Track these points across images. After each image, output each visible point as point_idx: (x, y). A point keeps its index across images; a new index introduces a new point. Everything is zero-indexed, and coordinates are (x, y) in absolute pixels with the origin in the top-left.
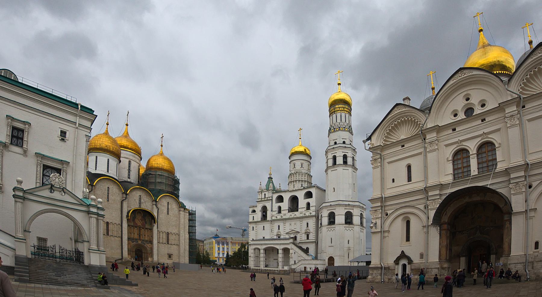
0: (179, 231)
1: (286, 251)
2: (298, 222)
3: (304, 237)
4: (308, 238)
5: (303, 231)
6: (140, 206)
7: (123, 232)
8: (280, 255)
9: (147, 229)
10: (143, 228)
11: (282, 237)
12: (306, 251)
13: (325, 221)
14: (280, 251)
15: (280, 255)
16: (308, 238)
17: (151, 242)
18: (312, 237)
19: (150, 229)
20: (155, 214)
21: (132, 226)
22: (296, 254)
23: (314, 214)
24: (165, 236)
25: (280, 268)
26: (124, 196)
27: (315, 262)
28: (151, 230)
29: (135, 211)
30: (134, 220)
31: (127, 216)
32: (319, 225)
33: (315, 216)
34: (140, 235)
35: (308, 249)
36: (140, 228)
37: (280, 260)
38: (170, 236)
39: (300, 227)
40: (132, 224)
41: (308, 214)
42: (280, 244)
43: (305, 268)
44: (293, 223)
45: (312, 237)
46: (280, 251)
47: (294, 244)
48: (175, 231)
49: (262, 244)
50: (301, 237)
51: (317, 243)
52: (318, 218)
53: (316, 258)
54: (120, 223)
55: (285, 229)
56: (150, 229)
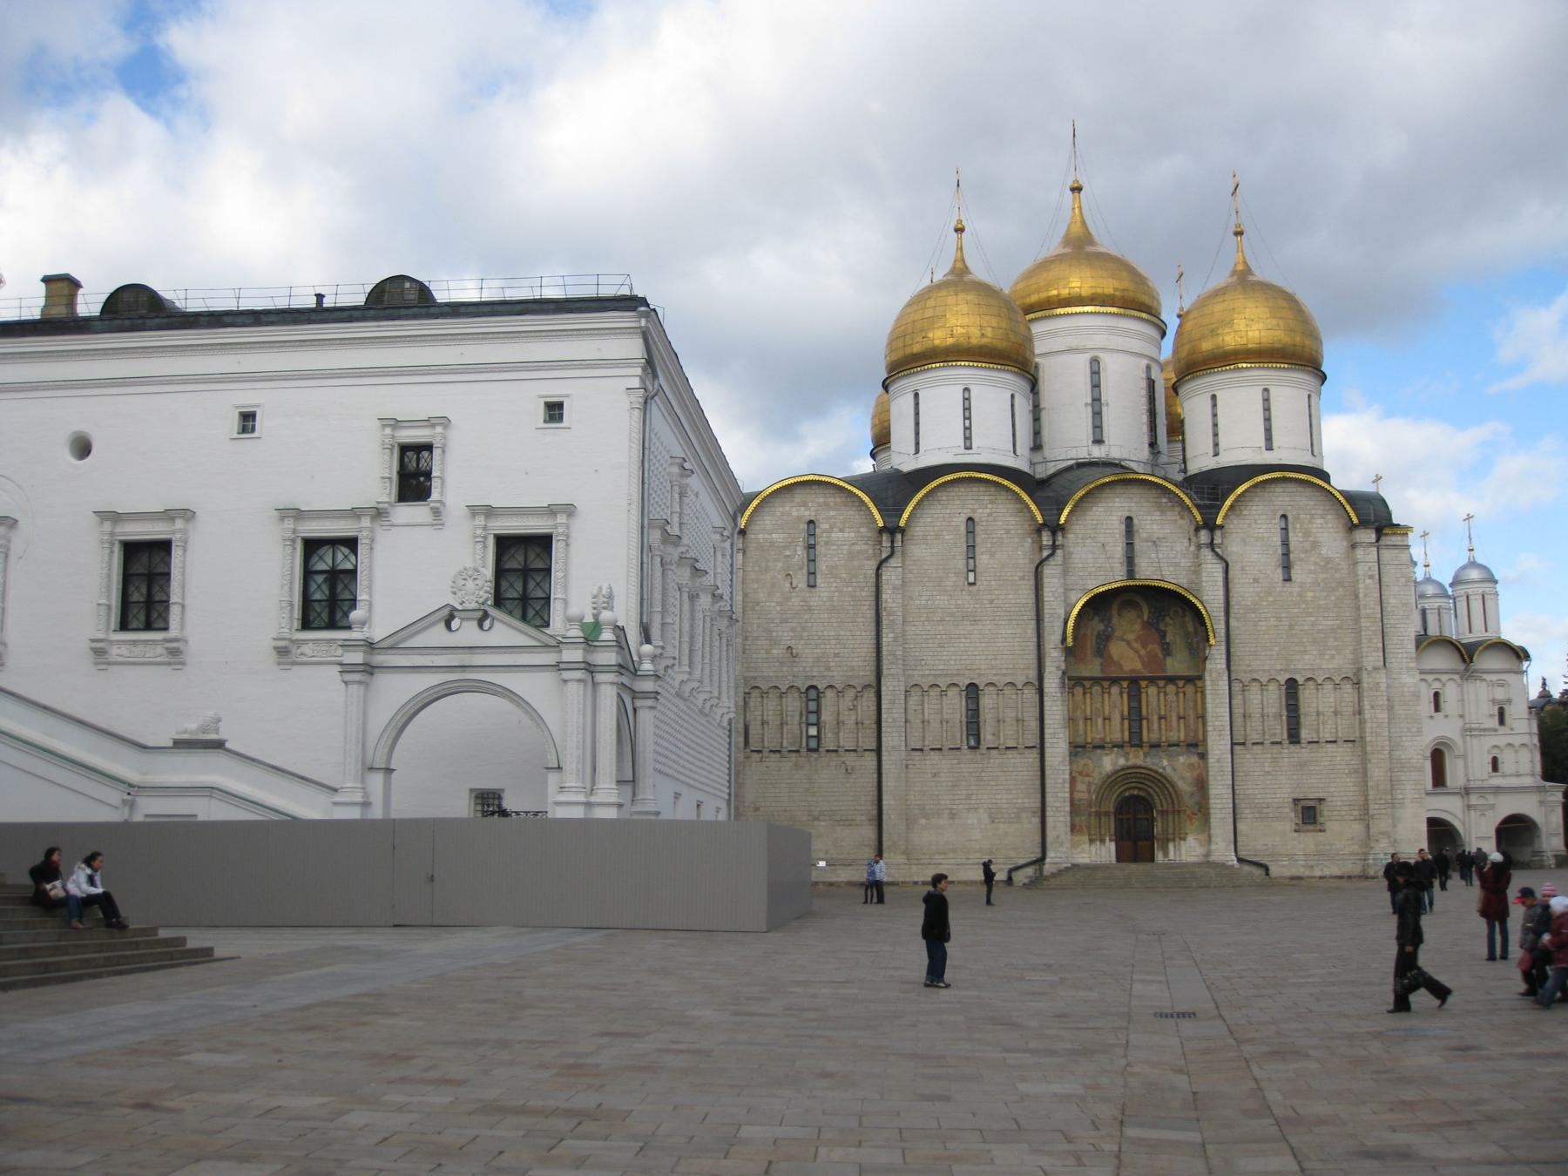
6: (1131, 573)
7: (1047, 722)
9: (1172, 680)
10: (1152, 680)
17: (1197, 746)
19: (1189, 680)
21: (1096, 680)
24: (1274, 699)
26: (1046, 539)
28: (1195, 680)
29: (1099, 604)
30: (1101, 651)
34: (1136, 717)
36: (1134, 681)
38: (1307, 697)
40: (1099, 674)
48: (1338, 663)
54: (1033, 674)
56: (1189, 680)
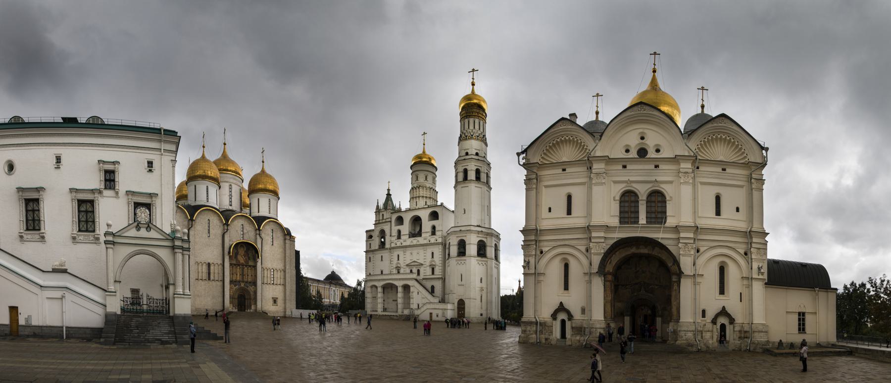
0: (285, 266)
1: (406, 288)
2: (421, 251)
3: (429, 271)
4: (433, 273)
5: (428, 264)
8: (400, 295)
11: (402, 271)
12: (432, 291)
13: (454, 250)
14: (400, 289)
15: (400, 295)
16: (433, 273)
18: (438, 271)
20: (259, 246)
22: (419, 296)
23: (440, 240)
25: (400, 312)
27: (442, 306)
31: (229, 253)
32: (446, 256)
33: (442, 243)
35: (433, 287)
37: (400, 301)
39: (422, 256)
41: (433, 240)
42: (400, 279)
43: (431, 314)
44: (415, 251)
45: (438, 271)
46: (400, 289)
47: (416, 280)
49: (379, 280)
50: (426, 272)
51: (443, 280)
52: (445, 246)
53: (443, 301)
55: (407, 258)
